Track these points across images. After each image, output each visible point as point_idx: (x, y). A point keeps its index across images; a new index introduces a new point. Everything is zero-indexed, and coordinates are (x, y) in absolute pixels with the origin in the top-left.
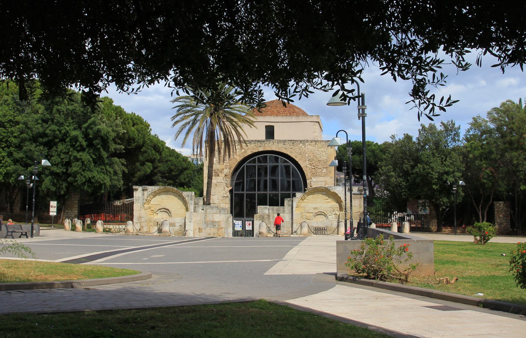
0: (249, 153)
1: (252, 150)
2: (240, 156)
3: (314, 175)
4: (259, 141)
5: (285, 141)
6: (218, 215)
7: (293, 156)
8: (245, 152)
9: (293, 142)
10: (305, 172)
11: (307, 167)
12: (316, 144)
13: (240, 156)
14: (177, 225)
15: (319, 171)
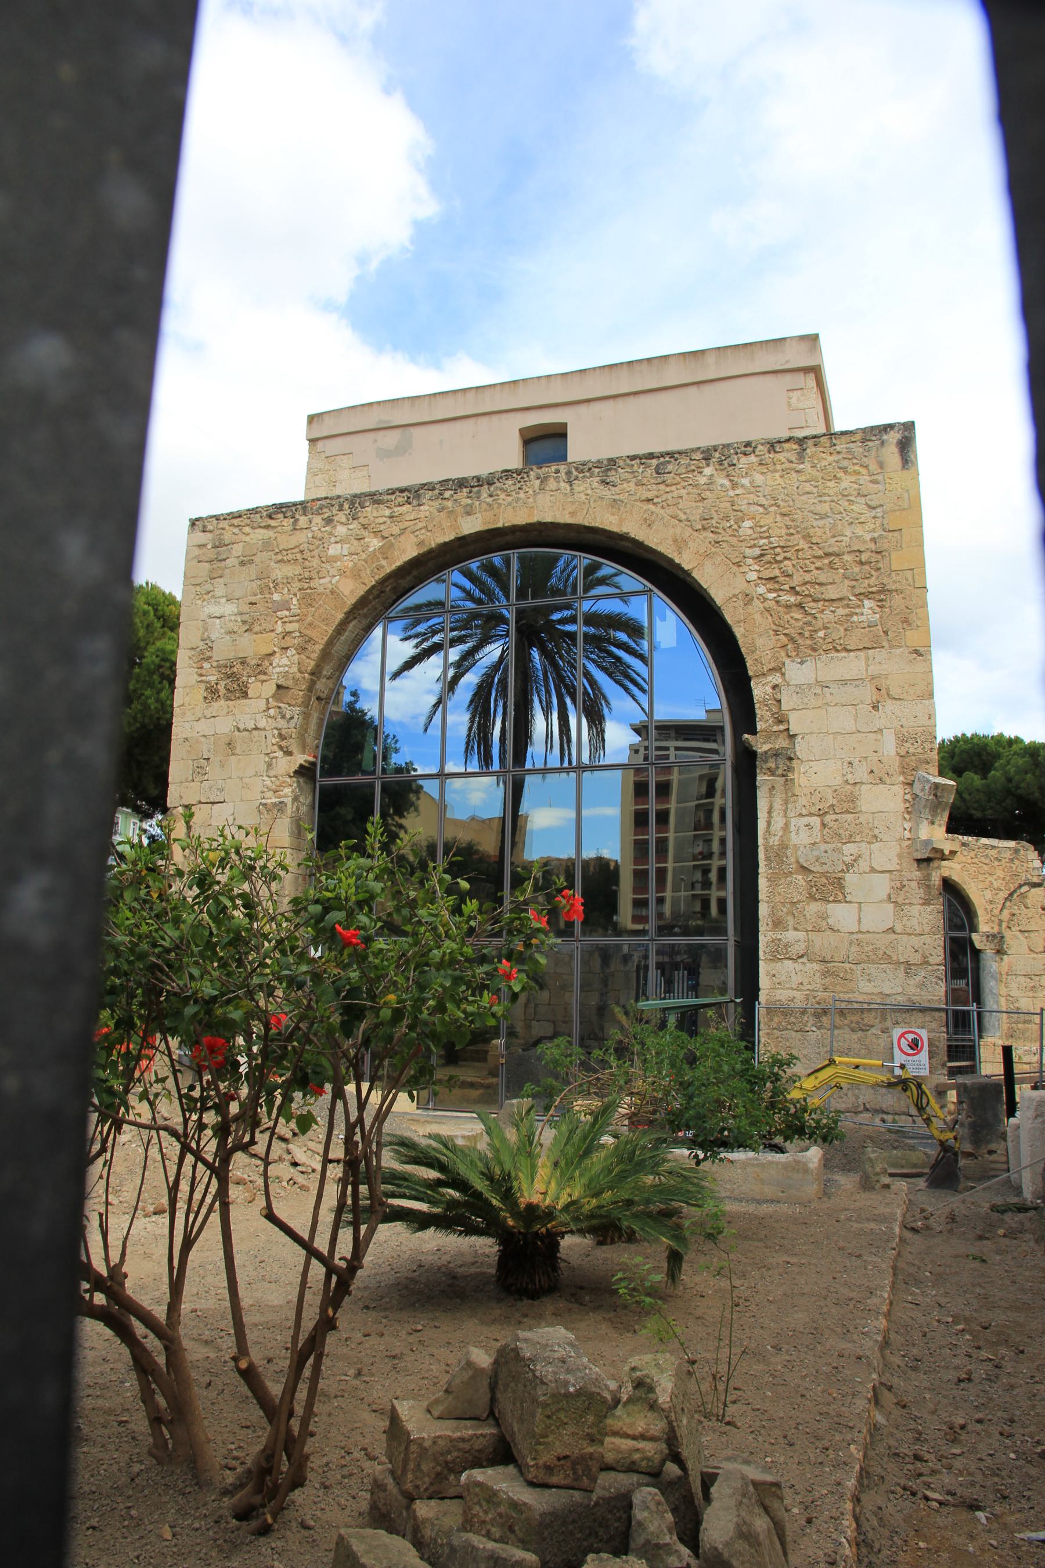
0: (408, 551)
1: (423, 535)
2: (356, 574)
3: (799, 644)
4: (461, 483)
5: (612, 462)
7: (658, 539)
8: (384, 552)
9: (660, 462)
10: (738, 631)
11: (748, 599)
12: (801, 456)
13: (356, 574)
15: (828, 616)
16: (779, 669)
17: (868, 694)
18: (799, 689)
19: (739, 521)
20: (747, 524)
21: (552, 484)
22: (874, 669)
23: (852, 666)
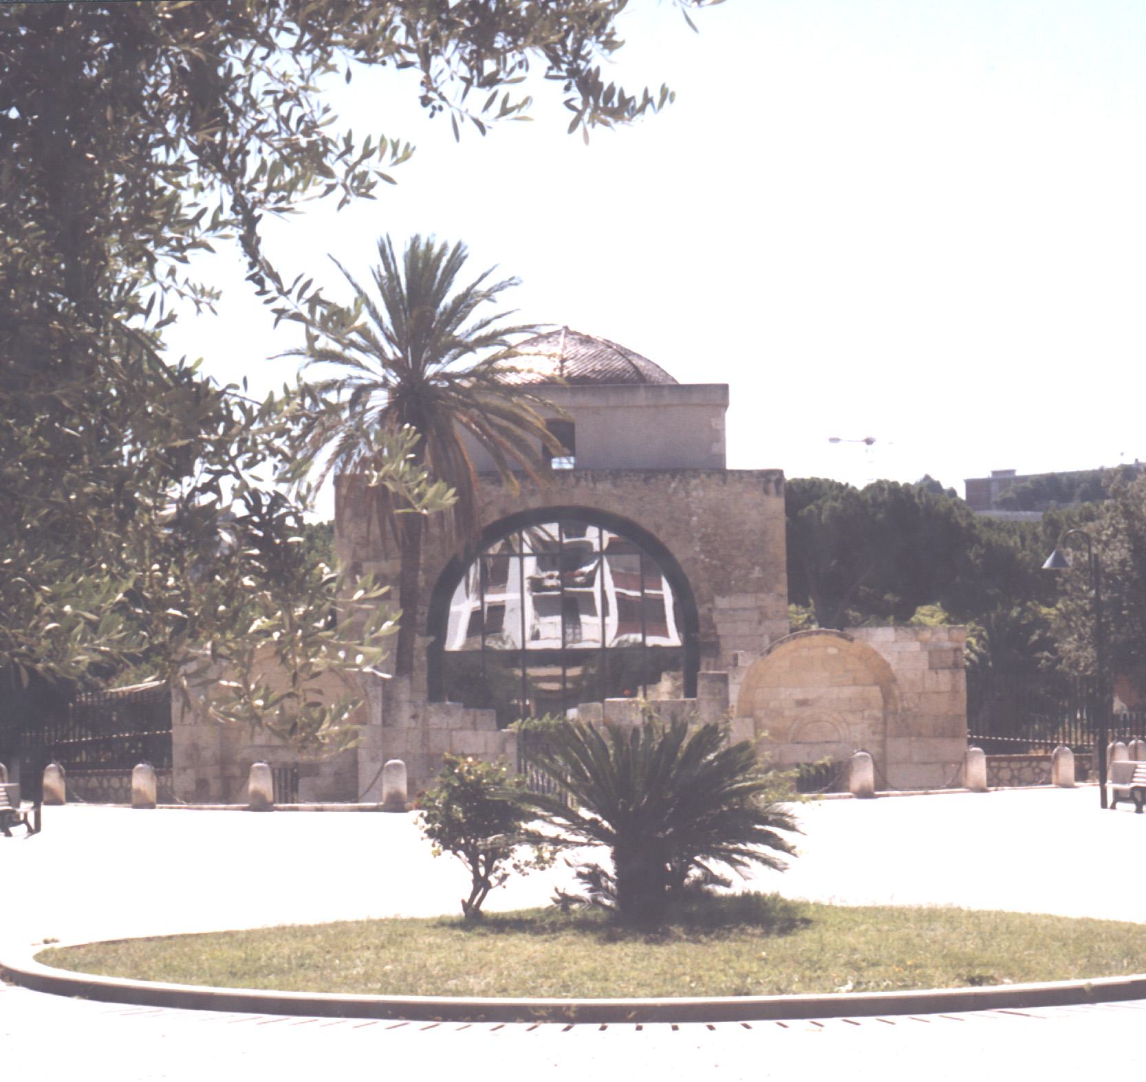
3: (722, 589)
6: (469, 733)
7: (646, 523)
10: (691, 579)
11: (695, 561)
14: (327, 770)
16: (712, 600)
17: (756, 616)
18: (722, 612)
19: (691, 515)
20: (695, 519)
21: (583, 483)
22: (760, 603)
23: (748, 601)
